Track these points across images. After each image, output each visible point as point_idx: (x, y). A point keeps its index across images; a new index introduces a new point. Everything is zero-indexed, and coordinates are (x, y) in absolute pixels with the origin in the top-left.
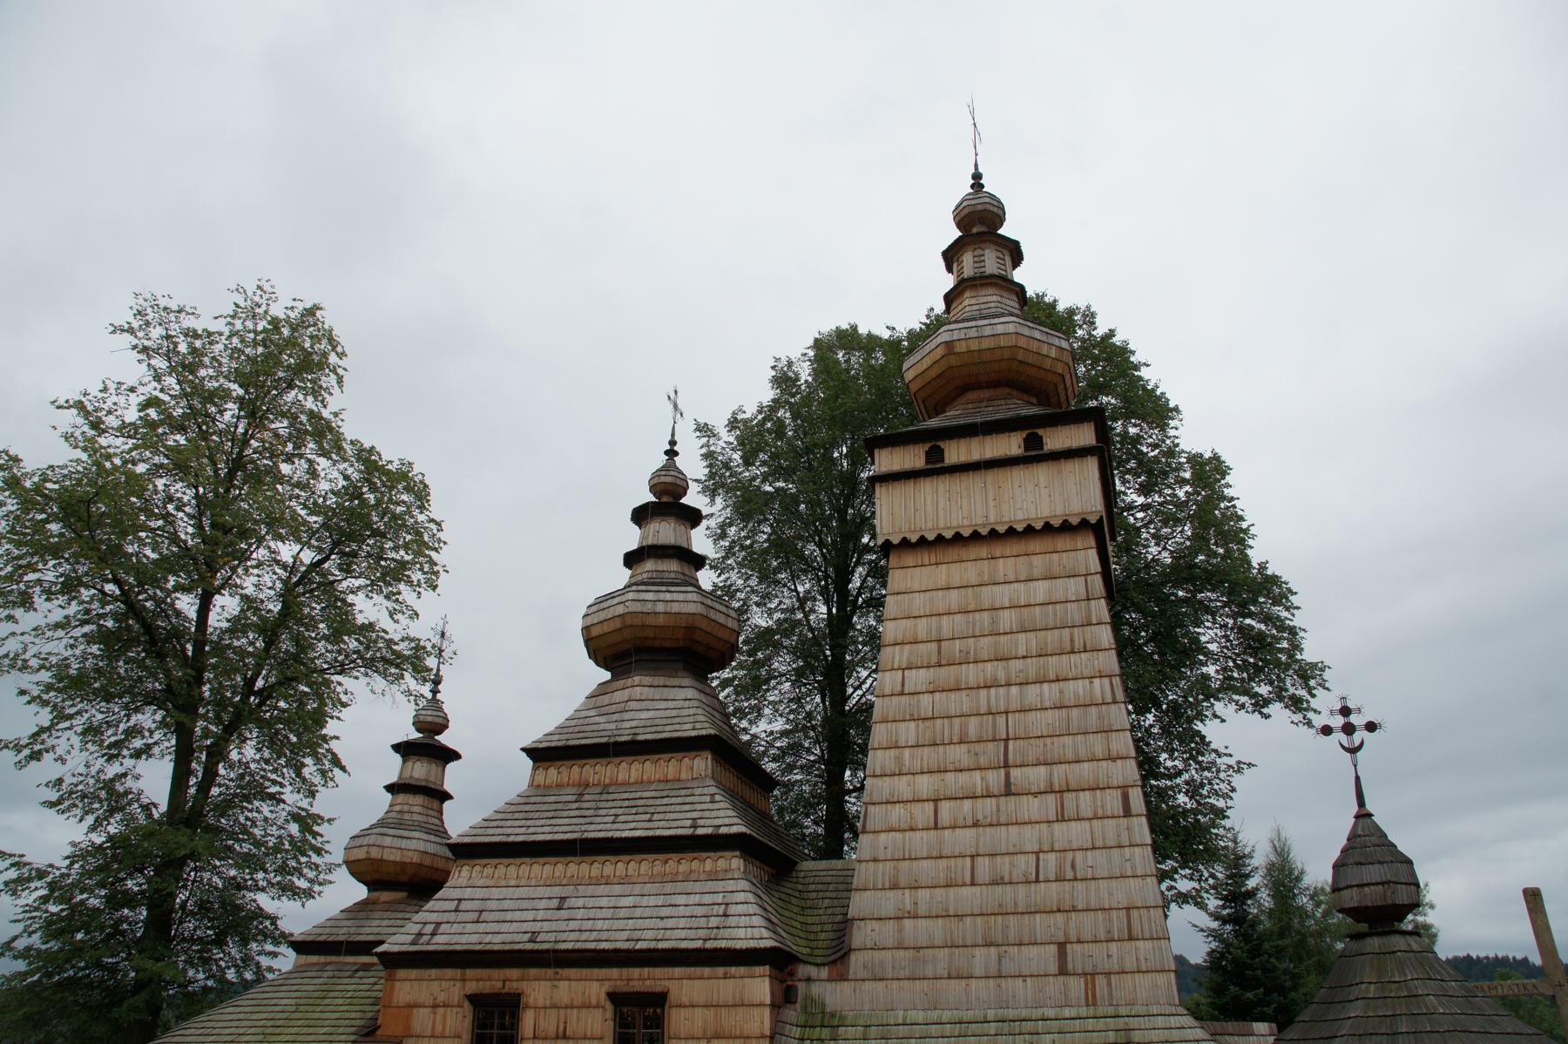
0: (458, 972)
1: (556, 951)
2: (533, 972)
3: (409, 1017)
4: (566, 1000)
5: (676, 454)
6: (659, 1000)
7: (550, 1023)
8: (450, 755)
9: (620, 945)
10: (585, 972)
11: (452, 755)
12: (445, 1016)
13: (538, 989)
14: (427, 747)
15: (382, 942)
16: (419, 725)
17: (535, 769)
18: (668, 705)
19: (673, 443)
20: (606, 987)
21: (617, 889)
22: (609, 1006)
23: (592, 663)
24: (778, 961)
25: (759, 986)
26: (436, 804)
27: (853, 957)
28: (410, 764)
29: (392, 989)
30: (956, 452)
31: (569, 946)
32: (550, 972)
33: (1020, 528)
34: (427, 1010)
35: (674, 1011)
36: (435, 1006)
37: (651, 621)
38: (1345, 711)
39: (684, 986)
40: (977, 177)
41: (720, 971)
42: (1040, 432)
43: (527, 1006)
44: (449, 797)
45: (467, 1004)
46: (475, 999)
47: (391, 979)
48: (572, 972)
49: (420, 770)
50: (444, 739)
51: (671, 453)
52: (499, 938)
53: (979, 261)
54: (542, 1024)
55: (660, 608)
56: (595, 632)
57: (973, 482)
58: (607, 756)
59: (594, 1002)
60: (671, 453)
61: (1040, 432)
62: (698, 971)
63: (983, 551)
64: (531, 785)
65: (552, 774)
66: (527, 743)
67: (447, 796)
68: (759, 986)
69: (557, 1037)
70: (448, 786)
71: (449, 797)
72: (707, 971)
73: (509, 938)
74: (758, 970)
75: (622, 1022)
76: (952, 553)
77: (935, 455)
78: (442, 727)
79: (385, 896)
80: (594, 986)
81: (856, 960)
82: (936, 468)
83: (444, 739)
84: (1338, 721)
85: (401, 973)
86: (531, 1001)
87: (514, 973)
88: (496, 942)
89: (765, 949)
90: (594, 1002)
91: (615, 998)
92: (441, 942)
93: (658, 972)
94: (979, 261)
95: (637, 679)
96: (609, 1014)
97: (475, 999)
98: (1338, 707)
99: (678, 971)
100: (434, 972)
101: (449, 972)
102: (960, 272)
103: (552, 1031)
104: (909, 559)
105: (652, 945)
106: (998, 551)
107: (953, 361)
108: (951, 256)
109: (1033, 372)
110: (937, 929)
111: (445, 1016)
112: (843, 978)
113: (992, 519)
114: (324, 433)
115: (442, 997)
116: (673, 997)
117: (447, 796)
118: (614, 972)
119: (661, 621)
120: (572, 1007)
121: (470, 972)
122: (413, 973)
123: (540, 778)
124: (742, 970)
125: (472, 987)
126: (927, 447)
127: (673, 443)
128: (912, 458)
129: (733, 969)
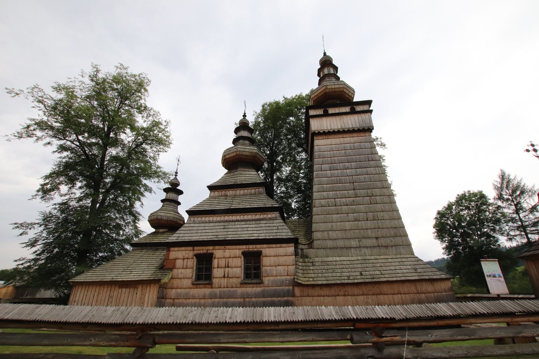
0: (192, 248)
1: (225, 240)
2: (217, 247)
3: (175, 262)
4: (228, 256)
5: (246, 116)
6: (259, 254)
7: (223, 262)
8: (181, 192)
9: (246, 238)
10: (234, 247)
11: (181, 192)
12: (187, 262)
13: (218, 252)
14: (174, 189)
17: (211, 192)
18: (250, 175)
19: (245, 113)
20: (242, 251)
21: (243, 223)
23: (224, 168)
25: (291, 249)
26: (176, 205)
27: (315, 242)
28: (169, 194)
29: (169, 254)
30: (331, 111)
31: (230, 239)
32: (223, 247)
34: (181, 260)
35: (264, 258)
36: (184, 259)
37: (244, 153)
38: (533, 145)
39: (267, 250)
41: (278, 245)
42: (355, 107)
43: (215, 258)
45: (195, 257)
46: (197, 256)
47: (169, 251)
48: (230, 247)
49: (172, 196)
51: (245, 116)
52: (205, 237)
53: (329, 71)
54: (220, 263)
55: (247, 150)
56: (227, 157)
57: (338, 118)
58: (234, 188)
59: (237, 256)
60: (245, 116)
61: (355, 107)
62: (271, 245)
63: (341, 136)
64: (210, 196)
65: (216, 193)
66: (209, 184)
67: (179, 204)
68: (291, 249)
69: (226, 267)
72: (274, 245)
73: (209, 237)
74: (291, 245)
75: (246, 261)
76: (332, 136)
78: (178, 185)
79: (161, 230)
80: (237, 251)
81: (316, 243)
82: (326, 114)
84: (531, 148)
85: (172, 249)
86: (216, 257)
87: (211, 248)
88: (205, 238)
89: (292, 238)
90: (237, 256)
91: (244, 254)
92: (187, 239)
93: (258, 246)
94: (329, 71)
95: (240, 169)
96: (243, 259)
97: (197, 256)
98: (530, 144)
99: (265, 246)
100: (183, 248)
101: (189, 248)
103: (224, 265)
104: (320, 138)
105: (257, 238)
106: (344, 136)
107: (327, 91)
108: (319, 71)
109: (347, 96)
110: (340, 234)
111: (187, 262)
112: (312, 248)
114: (141, 109)
115: (186, 256)
116: (264, 253)
117: (179, 204)
118: (244, 247)
119: (247, 154)
120: (230, 258)
121: (196, 248)
122: (176, 249)
123: (213, 194)
124: (285, 245)
125: (197, 252)
127: (245, 113)
128: (320, 112)
129: (283, 245)
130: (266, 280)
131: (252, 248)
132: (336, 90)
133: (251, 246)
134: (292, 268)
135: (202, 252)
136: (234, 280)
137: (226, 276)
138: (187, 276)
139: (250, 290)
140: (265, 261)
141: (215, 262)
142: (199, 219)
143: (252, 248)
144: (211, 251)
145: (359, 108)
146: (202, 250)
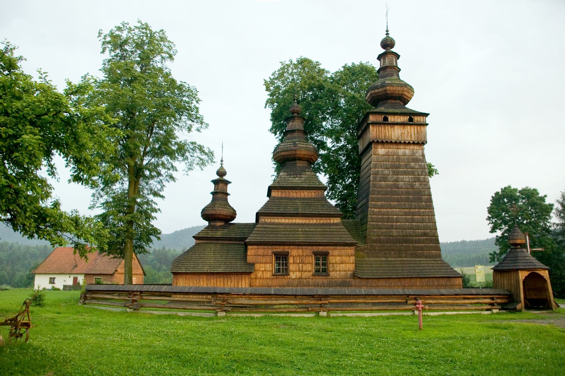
15: (247, 238)
16: (218, 173)
26: (225, 196)
30: (391, 119)
33: (407, 142)
40: (387, 31)
41: (342, 247)
44: (229, 195)
50: (225, 178)
70: (228, 192)
71: (229, 195)
75: (317, 259)
77: (386, 119)
82: (385, 122)
83: (225, 178)
87: (286, 247)
102: (384, 62)
116: (330, 254)
126: (383, 116)
130: (332, 274)
131: (321, 249)
132: (396, 92)
133: (321, 247)
134: (352, 267)
135: (279, 250)
137: (301, 269)
138: (268, 269)
139: (320, 280)
140: (331, 259)
141: (291, 260)
143: (321, 249)
144: (287, 250)
145: (416, 119)
146: (280, 249)
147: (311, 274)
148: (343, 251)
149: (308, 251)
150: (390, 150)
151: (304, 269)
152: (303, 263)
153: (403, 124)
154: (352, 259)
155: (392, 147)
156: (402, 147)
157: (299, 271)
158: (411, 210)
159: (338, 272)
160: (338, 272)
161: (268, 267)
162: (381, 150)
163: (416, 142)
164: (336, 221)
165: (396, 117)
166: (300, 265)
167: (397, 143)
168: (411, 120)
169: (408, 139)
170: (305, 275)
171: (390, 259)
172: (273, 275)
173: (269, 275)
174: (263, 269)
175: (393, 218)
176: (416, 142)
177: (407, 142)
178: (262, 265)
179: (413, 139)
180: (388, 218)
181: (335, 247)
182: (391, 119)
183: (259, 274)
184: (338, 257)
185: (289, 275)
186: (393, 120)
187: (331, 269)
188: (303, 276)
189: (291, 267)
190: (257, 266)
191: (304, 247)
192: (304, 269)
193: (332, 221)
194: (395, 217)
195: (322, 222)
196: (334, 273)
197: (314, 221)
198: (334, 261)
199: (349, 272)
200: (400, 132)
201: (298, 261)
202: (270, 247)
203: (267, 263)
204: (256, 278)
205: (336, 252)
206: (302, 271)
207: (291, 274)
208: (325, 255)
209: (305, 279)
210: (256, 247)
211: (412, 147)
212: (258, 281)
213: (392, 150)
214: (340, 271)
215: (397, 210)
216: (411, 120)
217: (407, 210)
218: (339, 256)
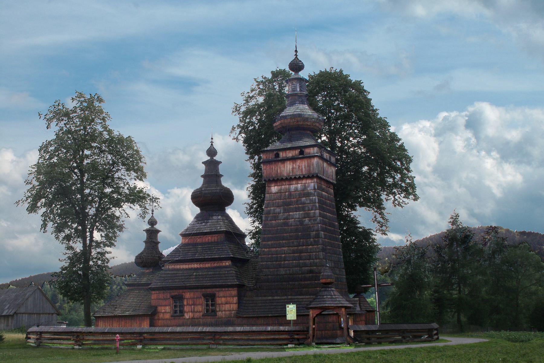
22: (203, 297)
24: (240, 287)
25: (234, 292)
33: (297, 177)
41: (227, 289)
43: (185, 298)
68: (234, 292)
77: (277, 155)
87: (181, 291)
93: (214, 290)
99: (217, 289)
113: (291, 174)
116: (217, 295)
125: (173, 294)
130: (219, 314)
131: (209, 291)
134: (235, 307)
136: (198, 314)
138: (167, 311)
139: (209, 320)
140: (219, 301)
142: (173, 266)
143: (209, 291)
147: (201, 314)
148: (227, 292)
149: (198, 293)
150: (283, 187)
151: (196, 310)
152: (194, 304)
153: (293, 159)
154: (235, 300)
155: (284, 184)
156: (294, 182)
157: (191, 312)
158: (300, 248)
159: (224, 312)
160: (224, 312)
161: (168, 309)
162: (274, 189)
163: (306, 176)
164: (227, 264)
165: (288, 151)
166: (193, 306)
167: (290, 179)
168: (302, 153)
169: (298, 173)
170: (197, 315)
171: (276, 298)
172: (172, 316)
173: (168, 316)
174: (163, 311)
175: (281, 257)
176: (306, 176)
177: (297, 177)
178: (163, 308)
179: (304, 173)
180: (277, 257)
181: (220, 289)
182: (282, 155)
183: (161, 316)
184: (223, 299)
185: (184, 316)
186: (284, 155)
187: (218, 310)
188: (195, 316)
189: (186, 309)
190: (159, 308)
191: (195, 290)
192: (196, 310)
193: (224, 264)
194: (283, 255)
195: (216, 265)
196: (220, 313)
197: (208, 265)
198: (220, 302)
199: (233, 312)
200: (291, 167)
201: (191, 303)
202: (168, 291)
203: (166, 306)
204: (159, 319)
205: (221, 294)
206: (194, 312)
207: (186, 314)
208: (213, 297)
209: (197, 318)
210: (157, 292)
211: (304, 181)
212: (160, 321)
213: (285, 186)
214: (225, 311)
215: (286, 248)
216: (302, 153)
217: (296, 248)
218: (224, 297)
